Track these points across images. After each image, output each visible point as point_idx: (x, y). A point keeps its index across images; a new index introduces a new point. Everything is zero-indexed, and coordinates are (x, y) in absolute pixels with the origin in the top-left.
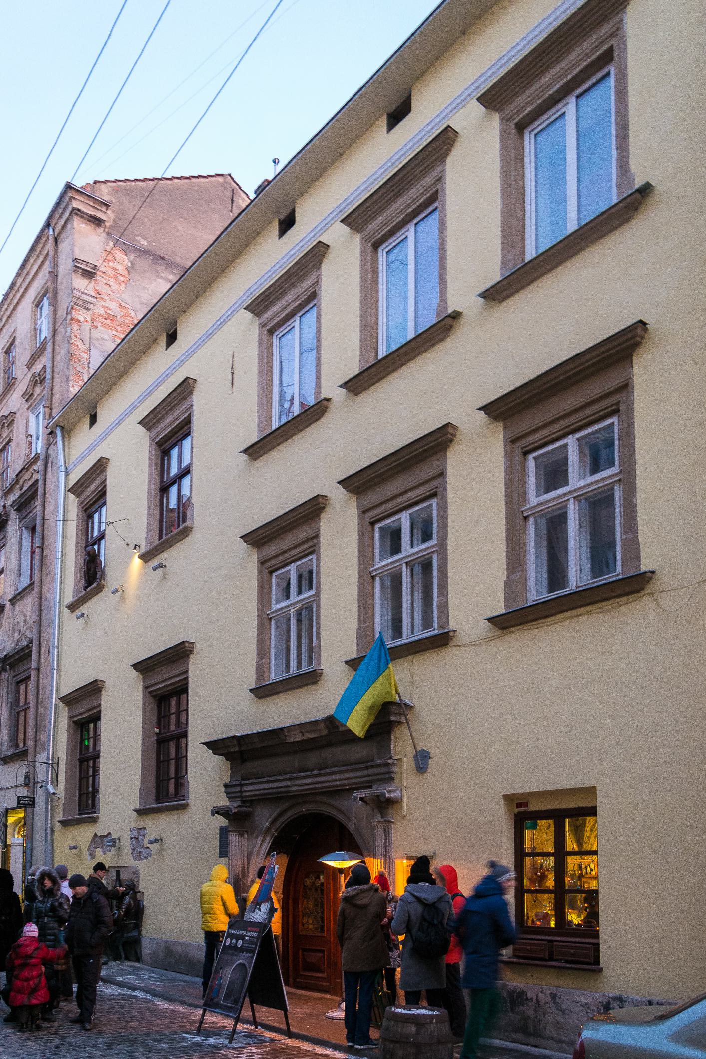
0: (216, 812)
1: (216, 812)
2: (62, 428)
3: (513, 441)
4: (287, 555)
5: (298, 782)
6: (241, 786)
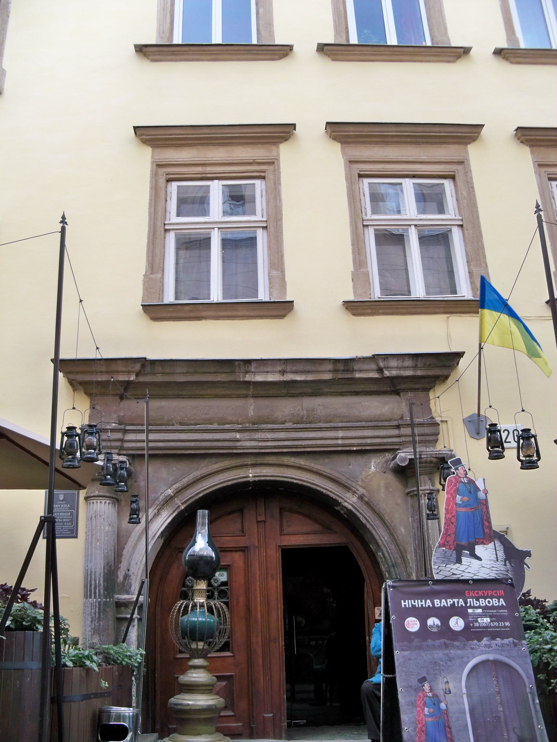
4: (209, 169)
5: (258, 435)
6: (125, 431)
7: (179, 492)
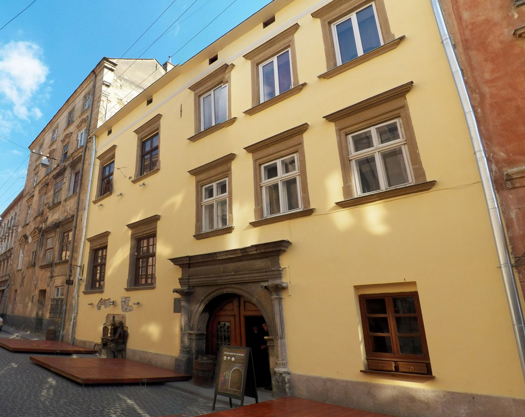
0: (176, 291)
1: (176, 291)
2: (96, 136)
3: (340, 130)
4: (211, 179)
5: (223, 278)
6: (189, 279)
7: (205, 297)
